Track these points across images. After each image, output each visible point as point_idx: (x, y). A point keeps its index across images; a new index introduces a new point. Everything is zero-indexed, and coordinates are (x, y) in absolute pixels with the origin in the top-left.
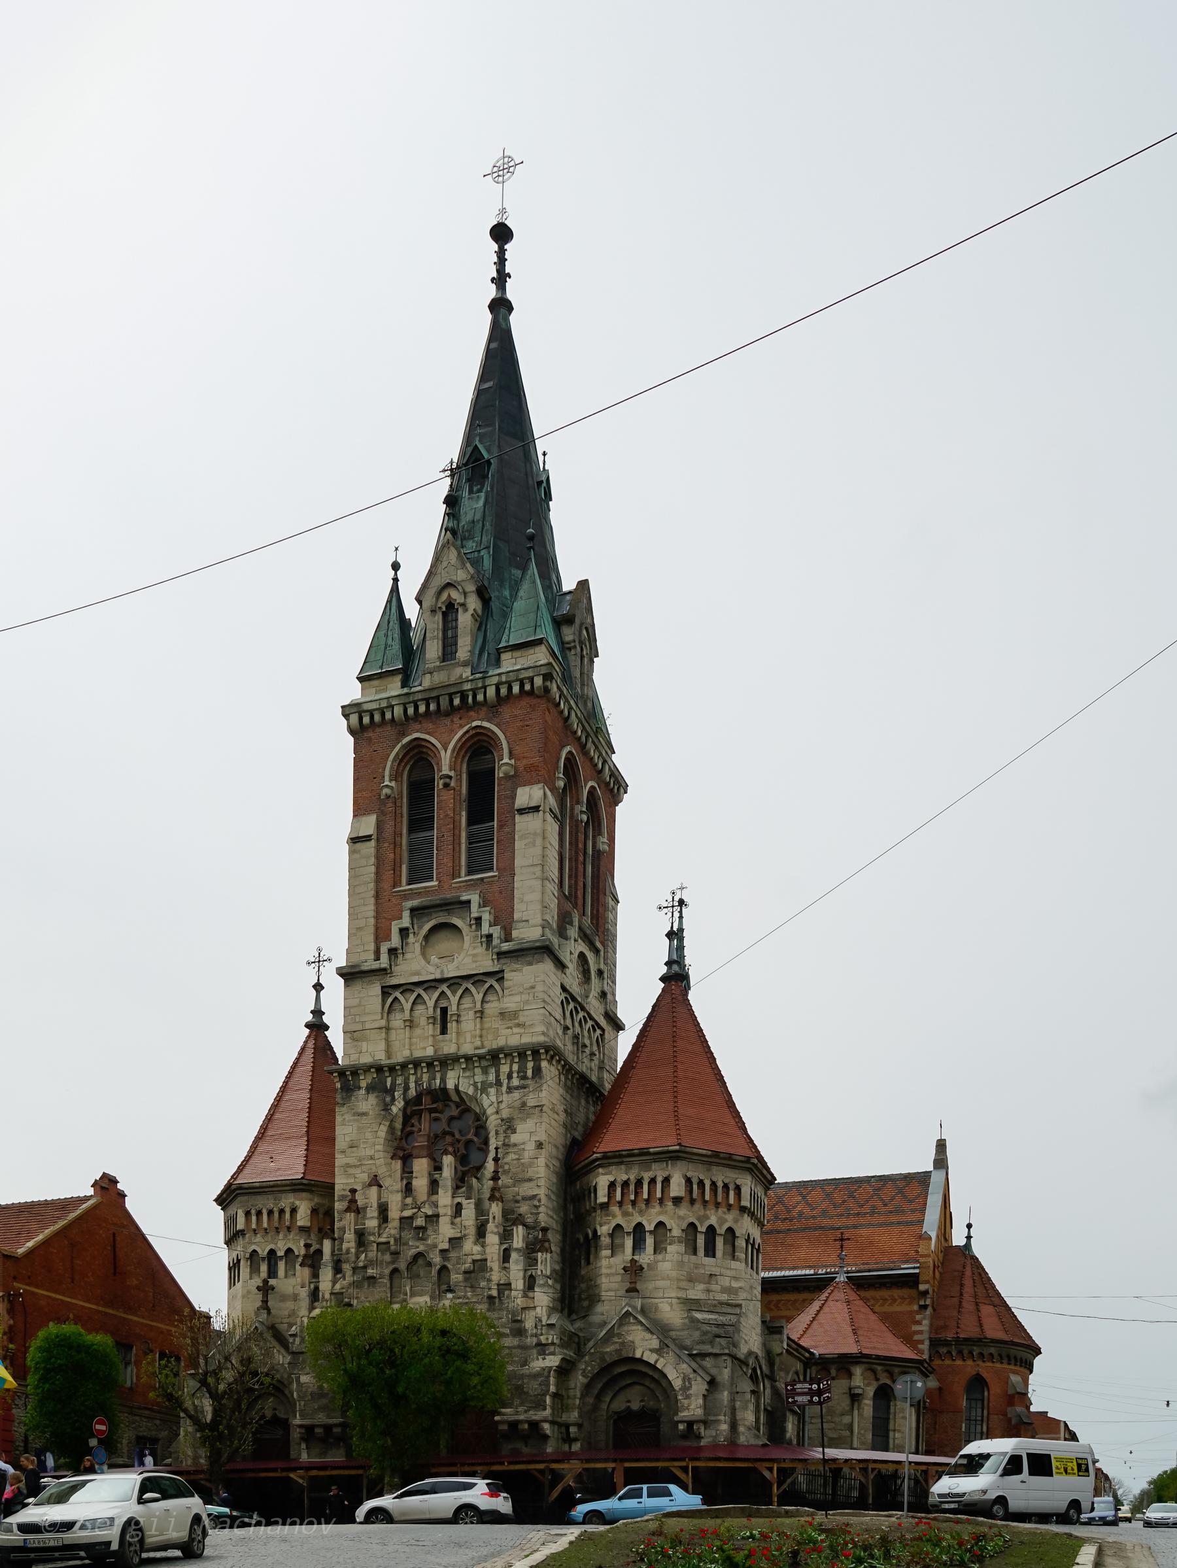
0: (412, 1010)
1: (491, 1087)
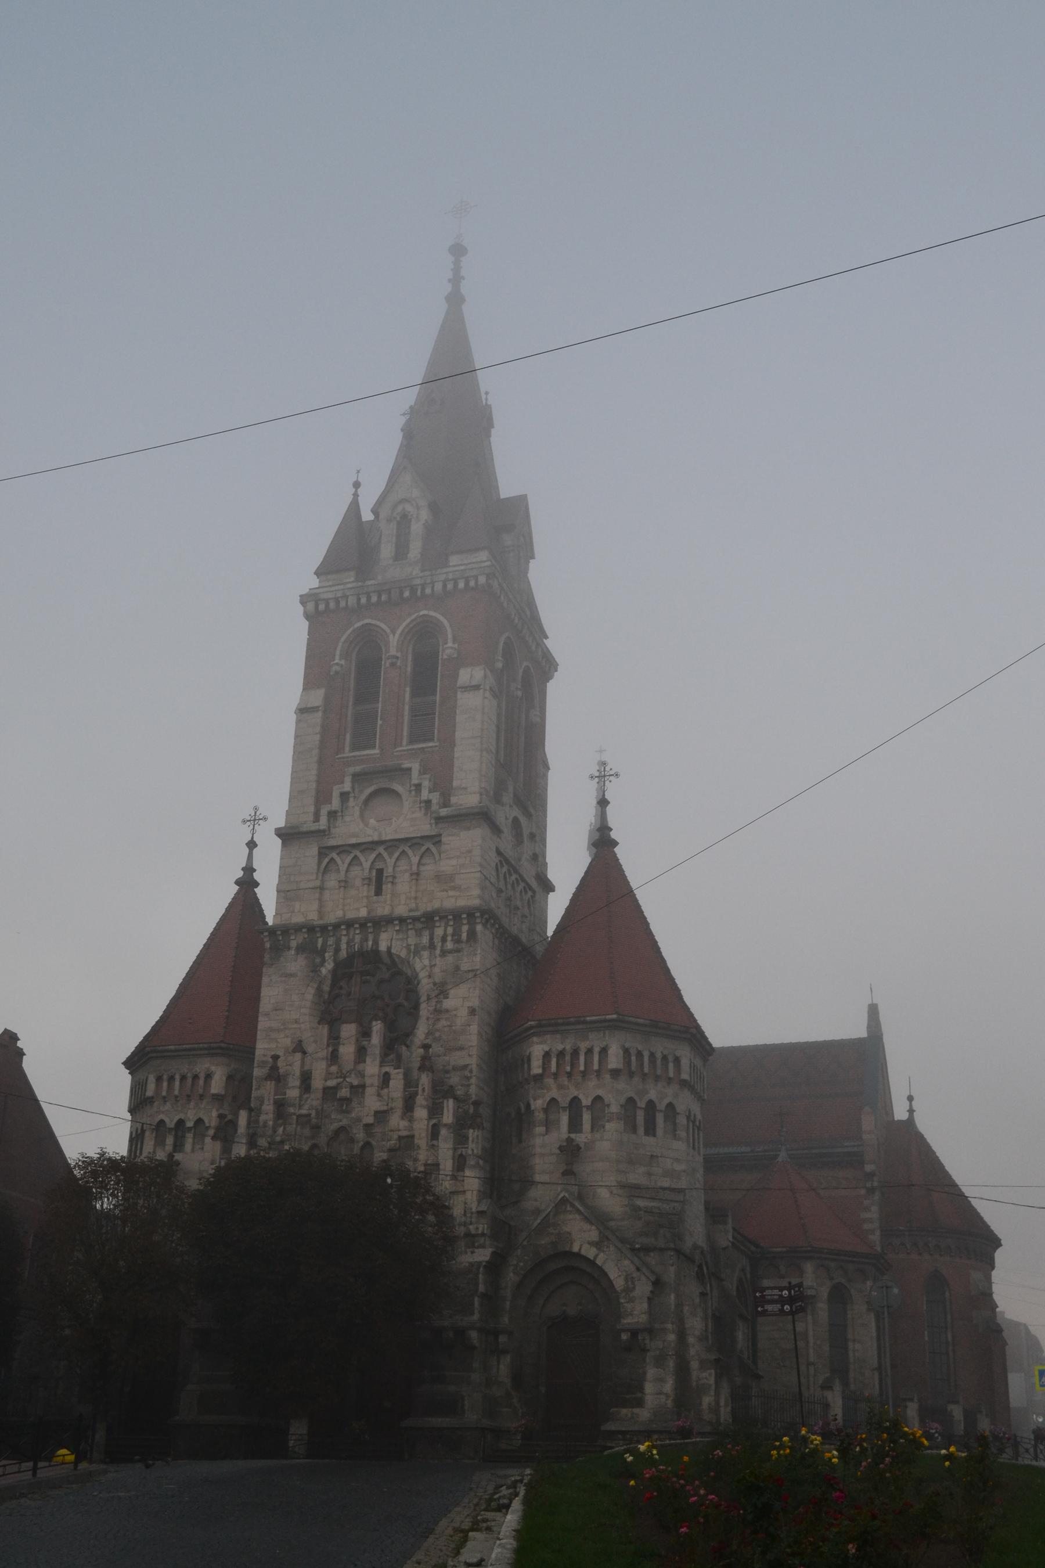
0: (347, 871)
1: (424, 948)
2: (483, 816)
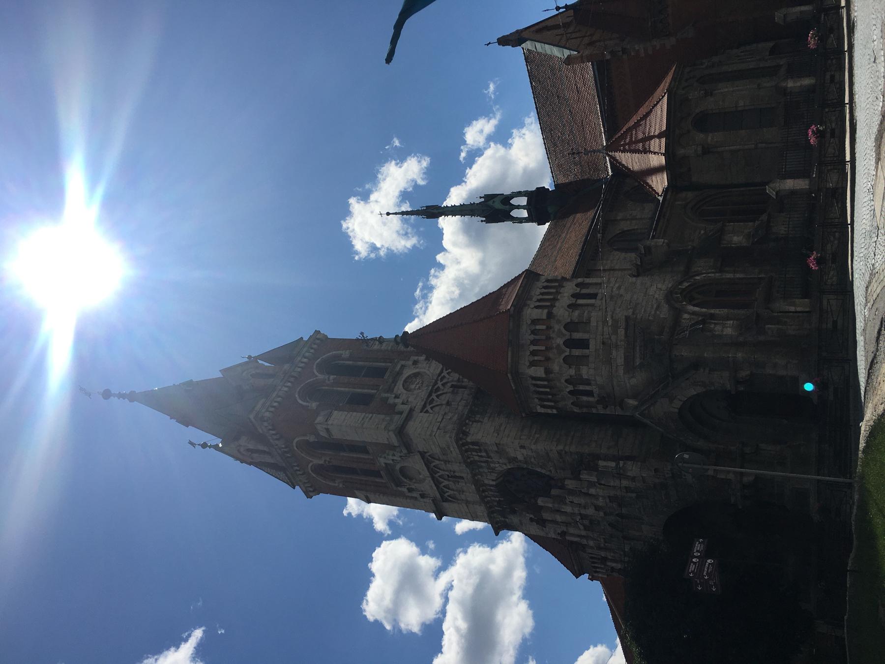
0: (453, 490)
2: (401, 432)
